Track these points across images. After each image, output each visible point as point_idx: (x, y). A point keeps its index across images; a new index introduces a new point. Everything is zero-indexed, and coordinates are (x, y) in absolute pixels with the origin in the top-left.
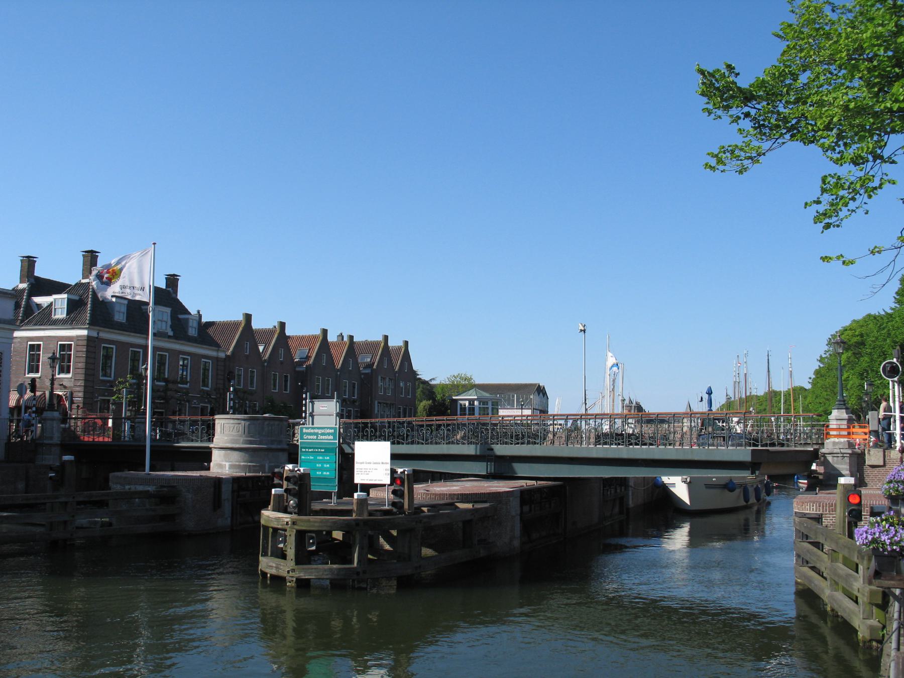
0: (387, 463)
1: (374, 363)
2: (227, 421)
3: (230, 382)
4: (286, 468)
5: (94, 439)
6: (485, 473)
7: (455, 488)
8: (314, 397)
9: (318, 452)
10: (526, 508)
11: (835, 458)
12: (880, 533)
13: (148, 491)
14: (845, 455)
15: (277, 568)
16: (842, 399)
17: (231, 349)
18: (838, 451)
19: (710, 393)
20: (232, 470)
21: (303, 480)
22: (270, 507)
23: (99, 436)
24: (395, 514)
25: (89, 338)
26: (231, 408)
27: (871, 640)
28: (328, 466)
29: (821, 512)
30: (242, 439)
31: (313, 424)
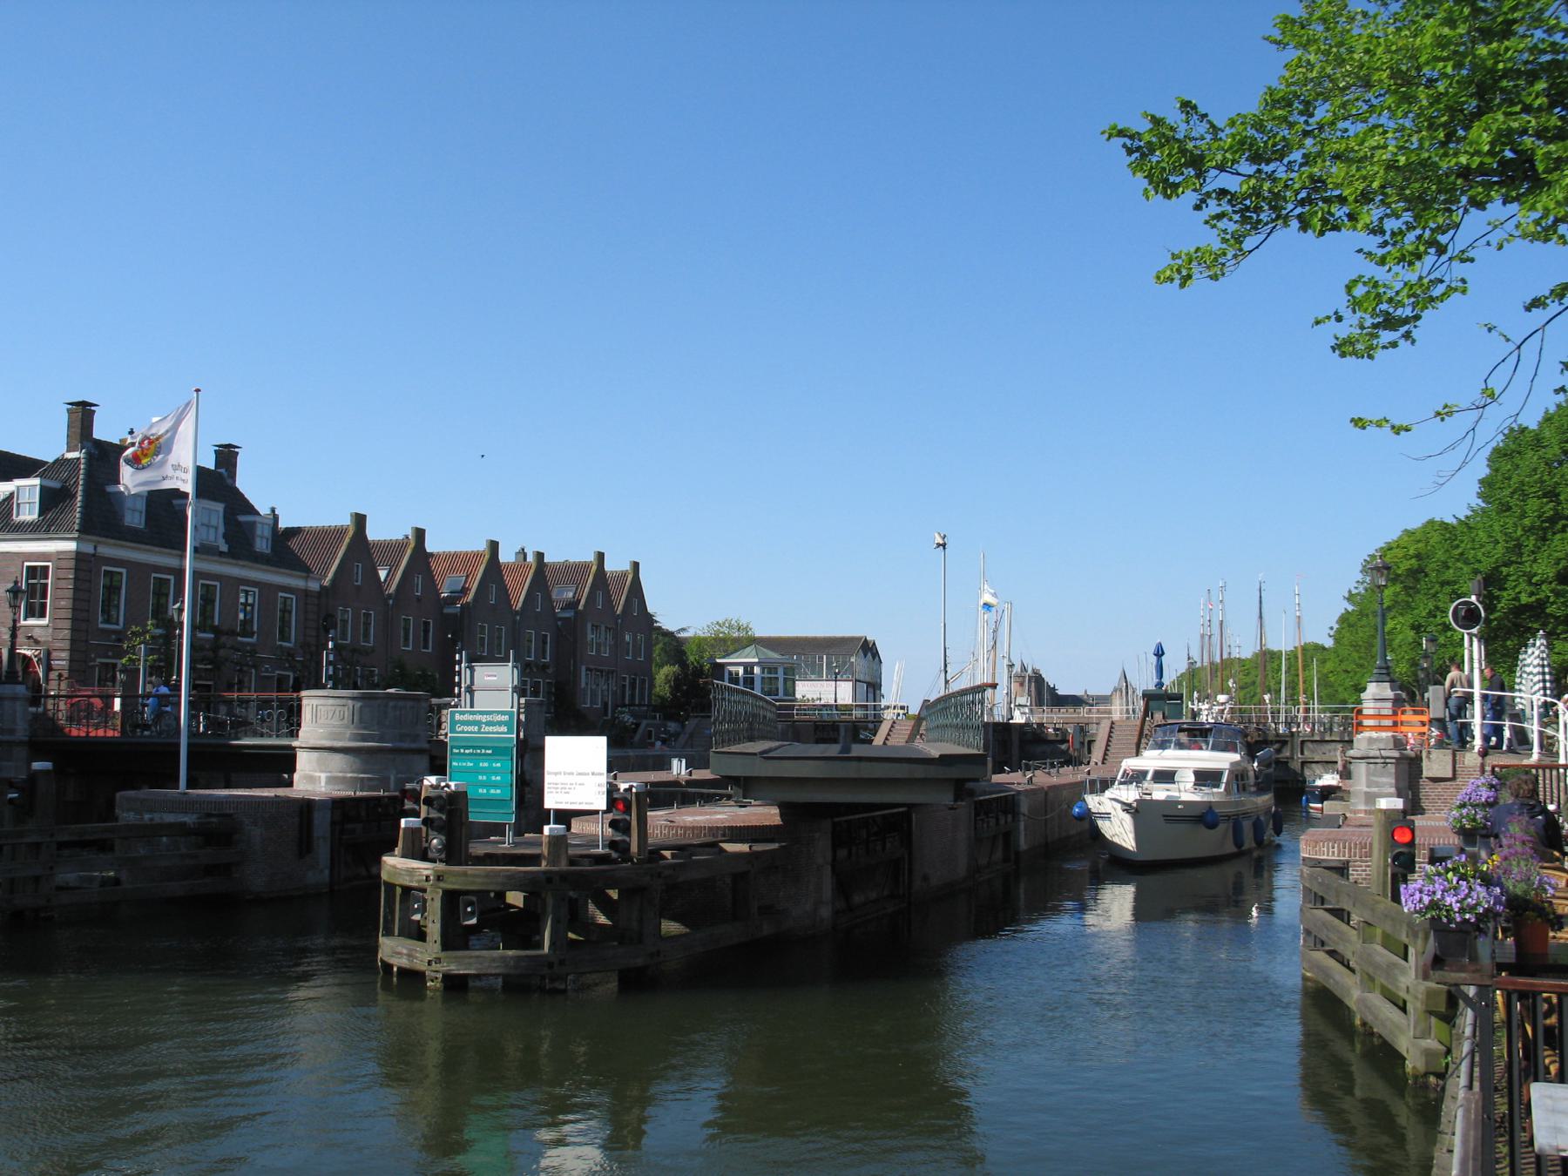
0: (601, 774)
2: (322, 701)
4: (426, 782)
5: (88, 732)
7: (718, 817)
8: (473, 659)
9: (480, 754)
10: (842, 853)
12: (1443, 891)
13: (184, 824)
14: (1388, 761)
15: (409, 955)
16: (1384, 665)
17: (330, 575)
18: (1377, 753)
19: (1159, 653)
20: (331, 787)
21: (453, 806)
22: (397, 851)
23: (97, 727)
24: (614, 861)
25: (79, 556)
26: (329, 678)
27: (1426, 1074)
28: (499, 778)
29: (1347, 858)
30: (348, 733)
31: (472, 706)
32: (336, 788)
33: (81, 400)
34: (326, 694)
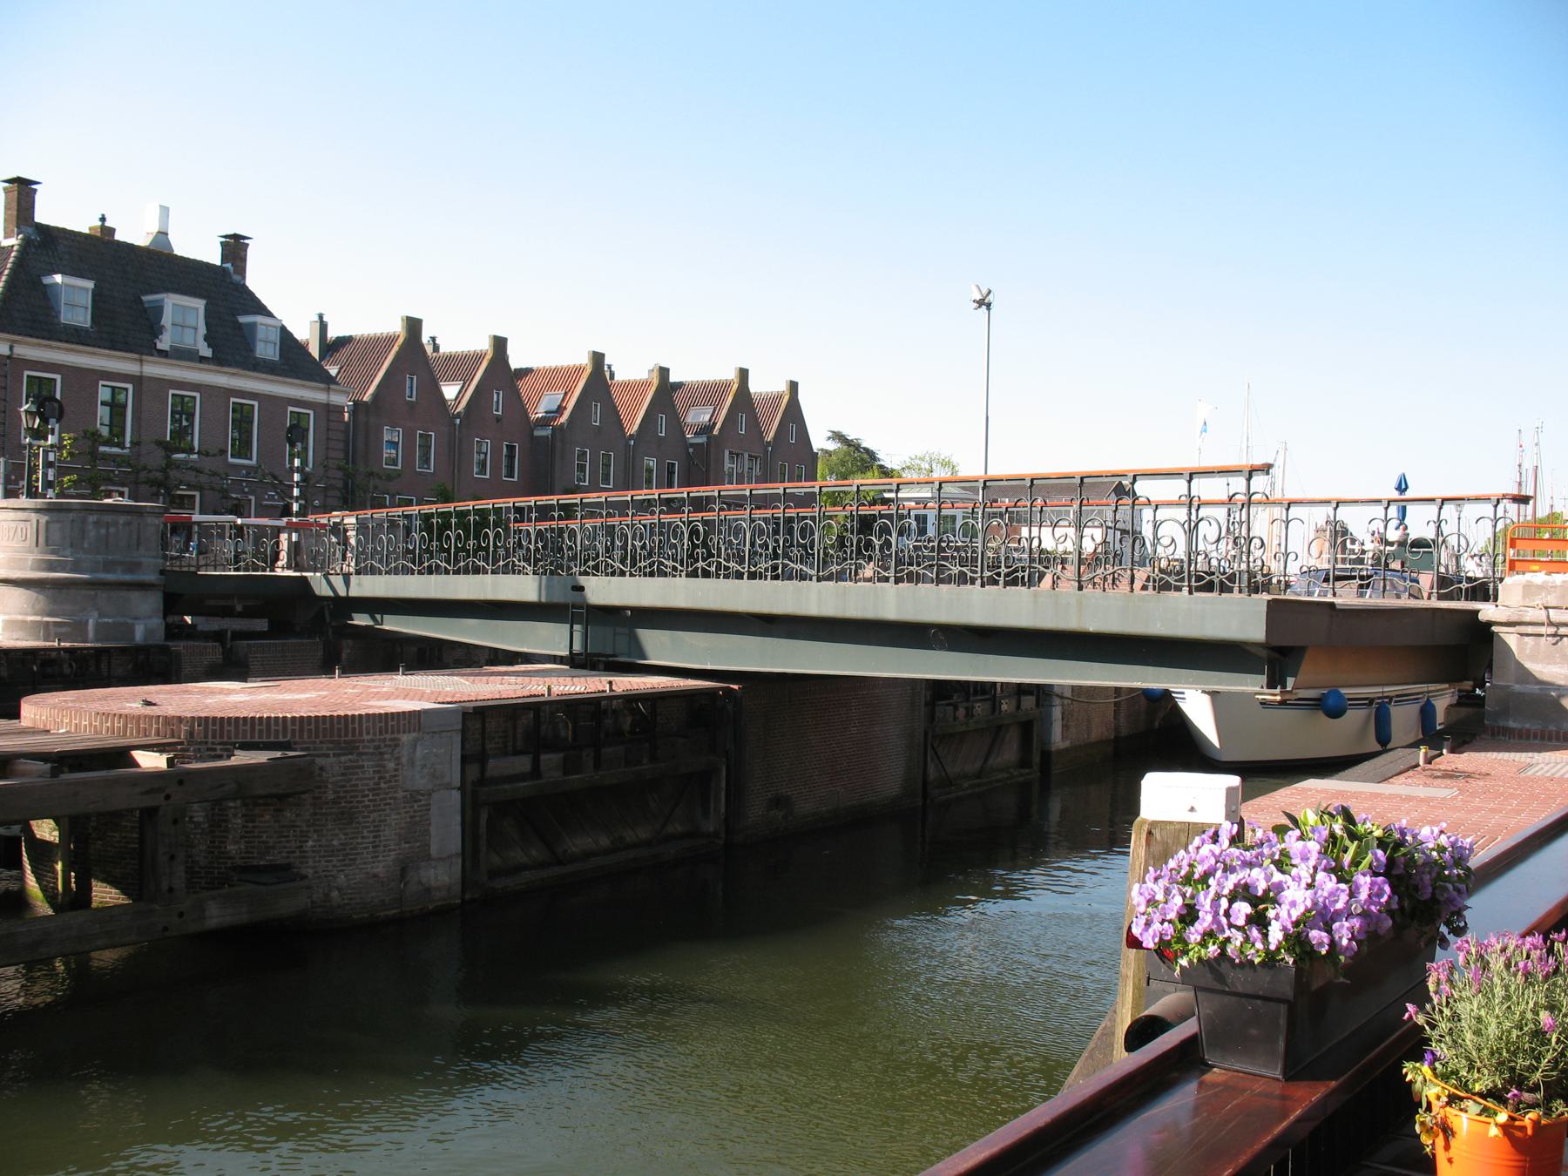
1: (715, 424)
3: (47, 423)
6: (566, 653)
11: (1526, 639)
18: (1541, 615)
30: (31, 557)
32: (15, 636)
33: (15, 176)
34: (5, 506)
